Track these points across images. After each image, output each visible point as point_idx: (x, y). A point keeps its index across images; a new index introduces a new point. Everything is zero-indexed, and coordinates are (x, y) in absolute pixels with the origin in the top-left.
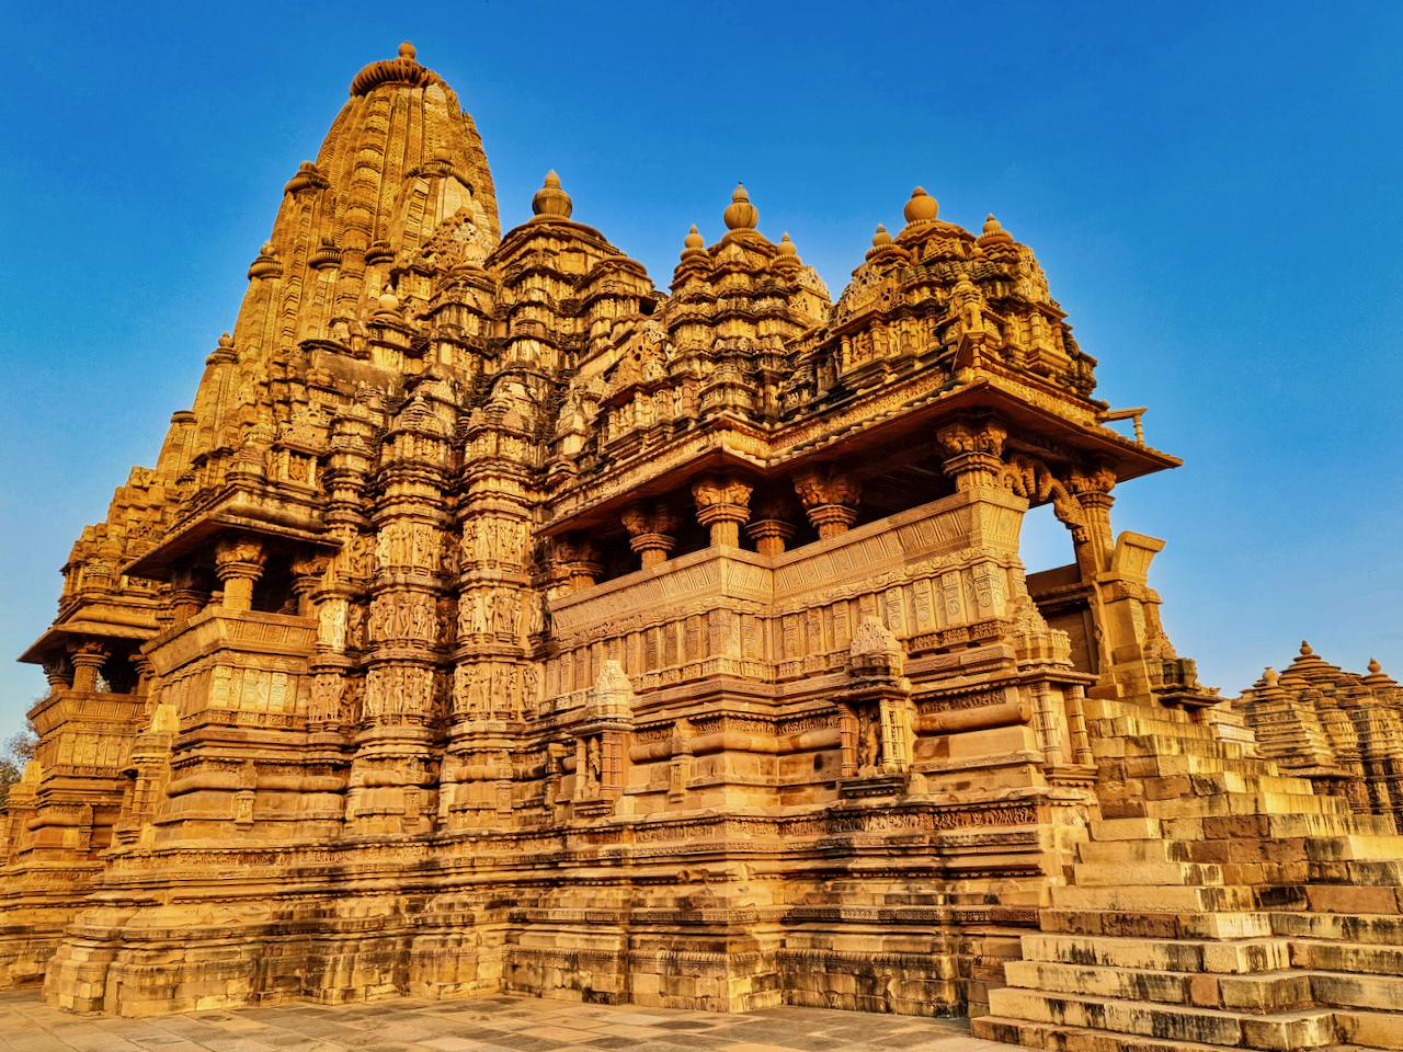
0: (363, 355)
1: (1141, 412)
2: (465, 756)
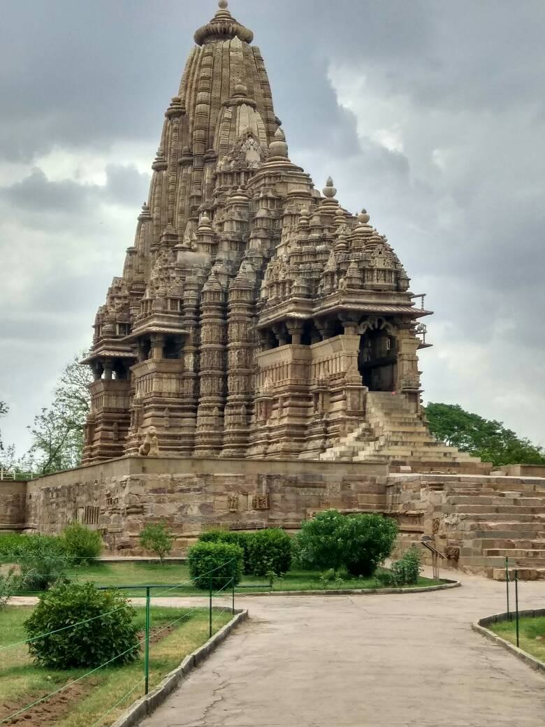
1: (425, 295)
2: (232, 407)
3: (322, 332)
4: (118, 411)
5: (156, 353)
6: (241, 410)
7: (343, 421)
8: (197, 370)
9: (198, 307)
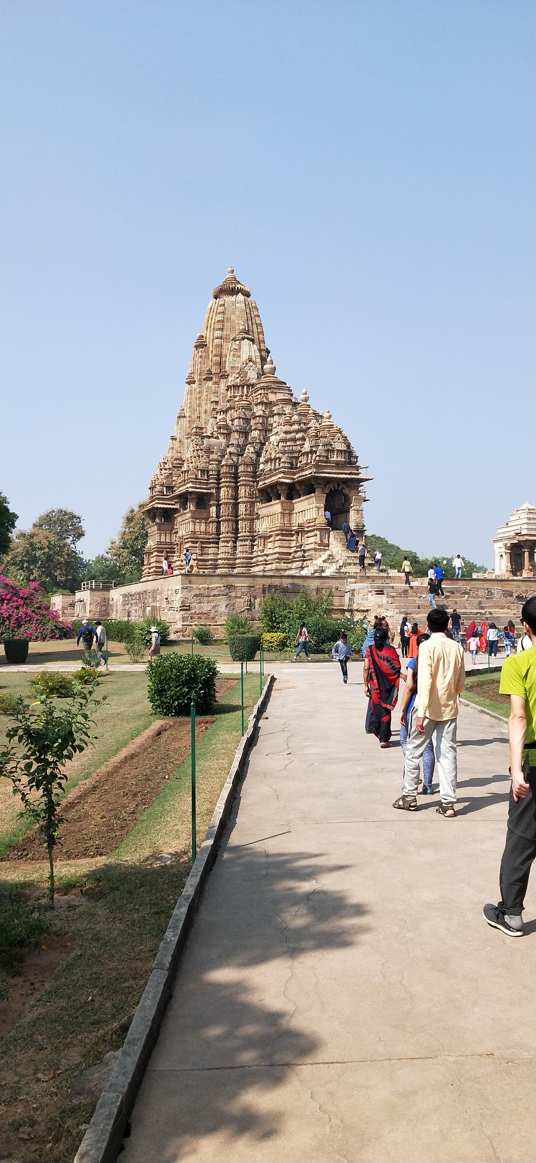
0: (217, 438)
2: (242, 540)
3: (300, 492)
4: (166, 543)
5: (191, 507)
6: (247, 543)
7: (315, 550)
8: (218, 516)
9: (218, 475)
